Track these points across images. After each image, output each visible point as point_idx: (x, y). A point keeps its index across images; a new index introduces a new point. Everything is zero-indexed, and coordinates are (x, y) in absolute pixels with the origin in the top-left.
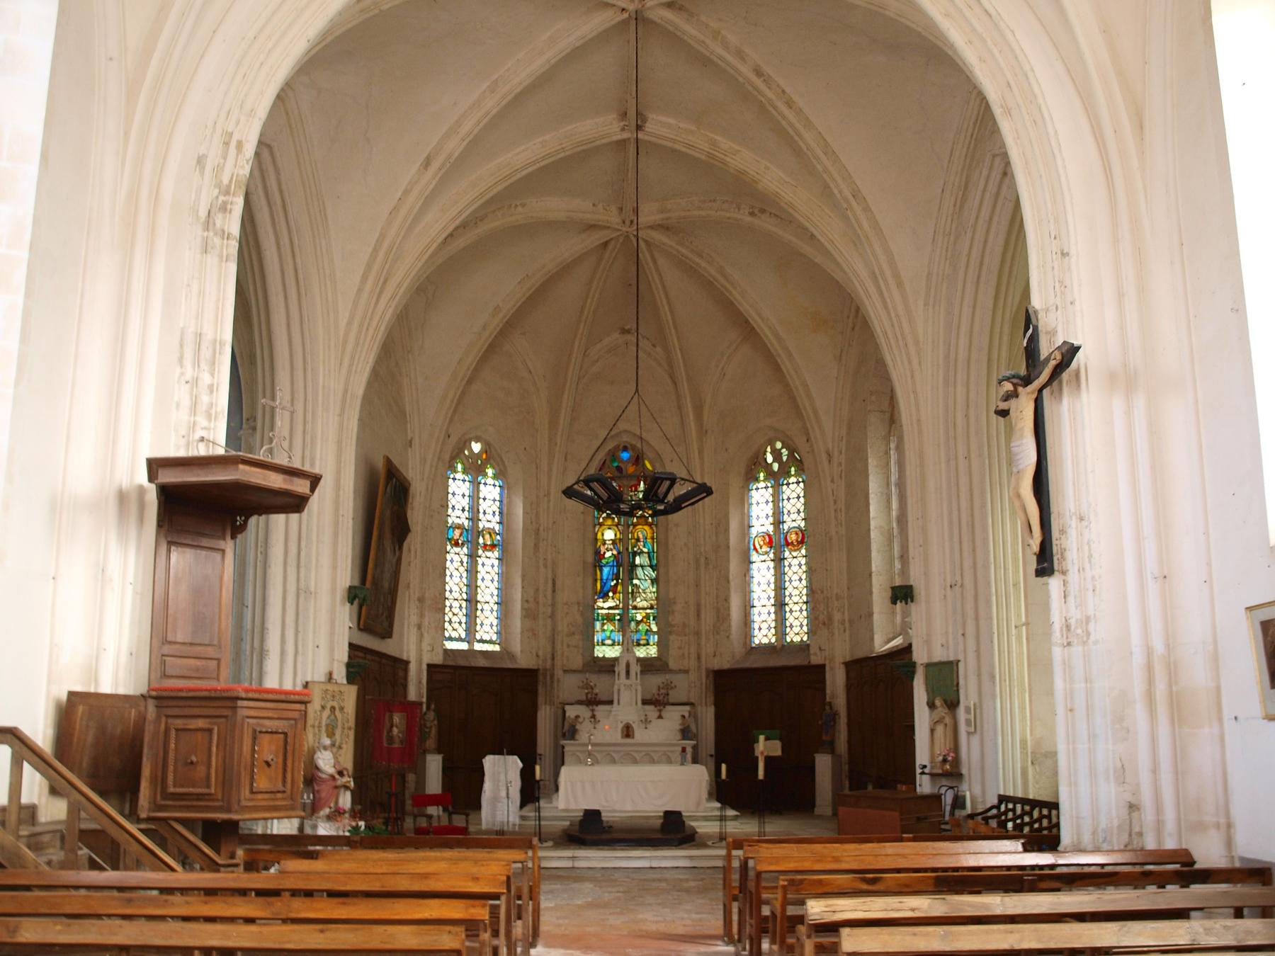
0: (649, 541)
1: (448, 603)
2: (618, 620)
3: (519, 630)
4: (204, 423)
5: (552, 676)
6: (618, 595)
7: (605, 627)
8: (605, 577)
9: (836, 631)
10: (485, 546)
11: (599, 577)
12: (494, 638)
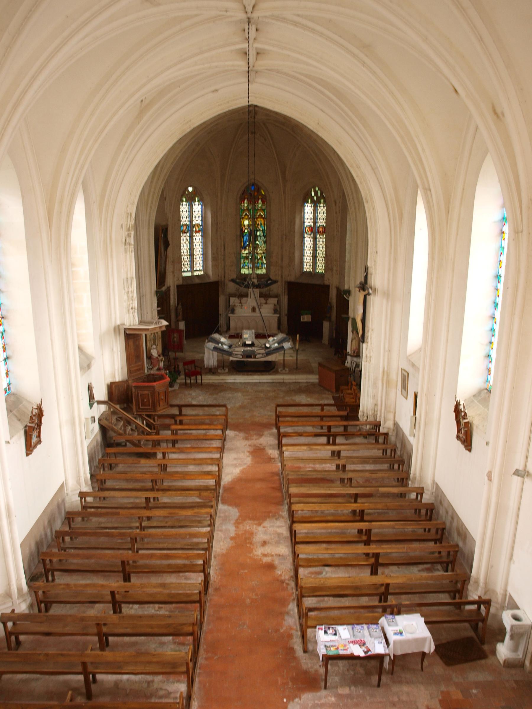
0: (263, 225)
1: (182, 258)
2: (250, 258)
4: (131, 302)
5: (224, 284)
12: (201, 269)
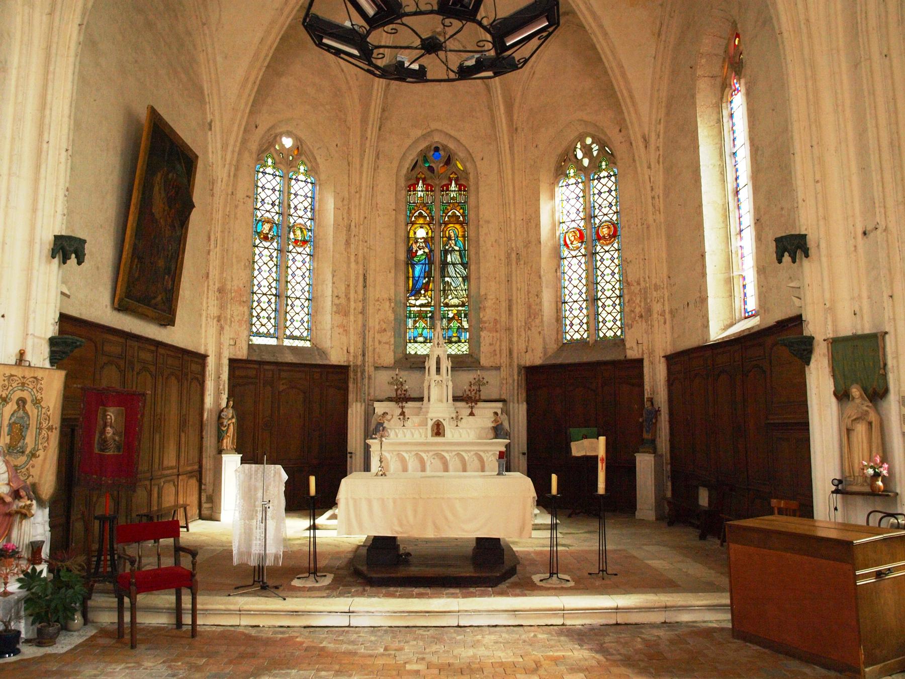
2: (430, 317)
3: (329, 326)
5: (363, 372)
6: (430, 292)
7: (417, 325)
8: (417, 274)
9: (656, 324)
10: (296, 241)
11: (411, 275)
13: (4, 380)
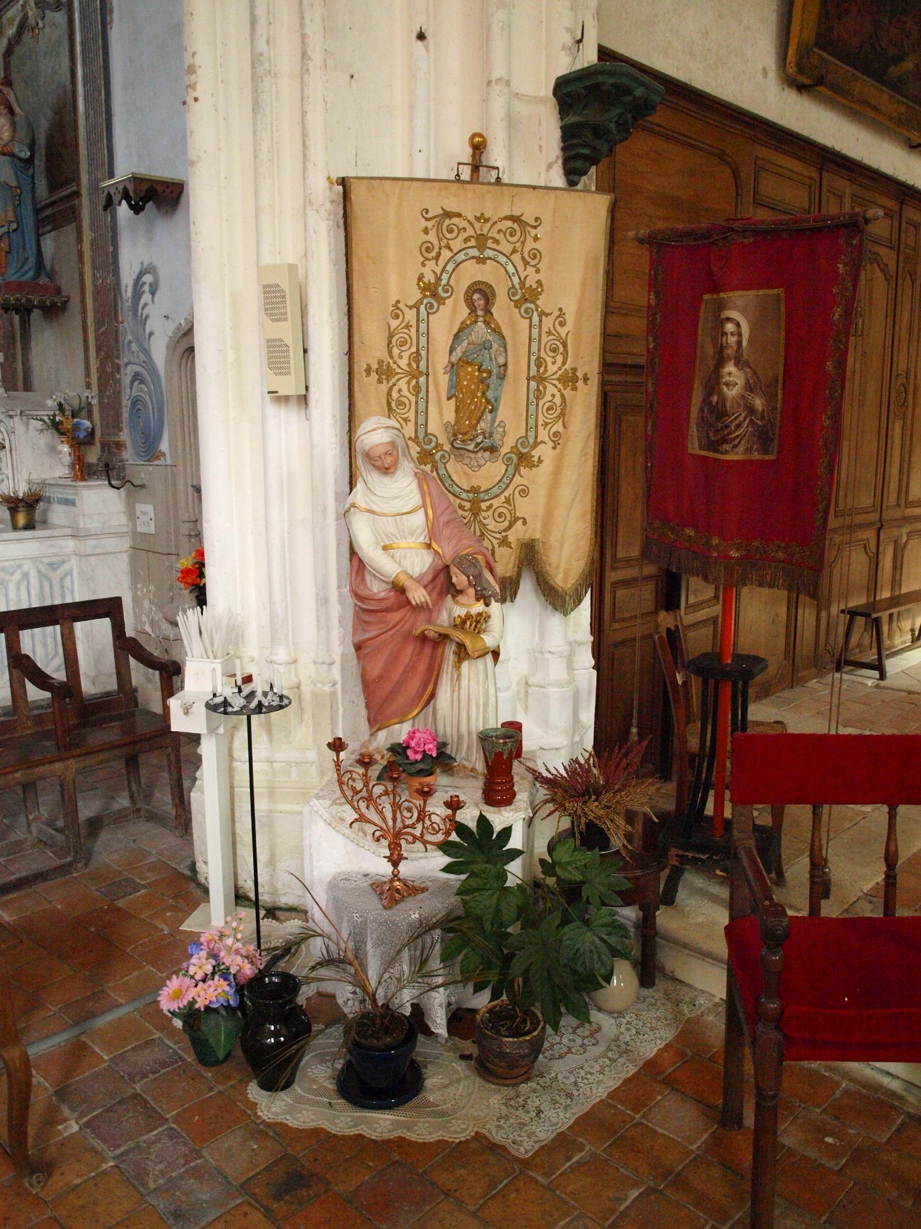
13: (426, 231)
